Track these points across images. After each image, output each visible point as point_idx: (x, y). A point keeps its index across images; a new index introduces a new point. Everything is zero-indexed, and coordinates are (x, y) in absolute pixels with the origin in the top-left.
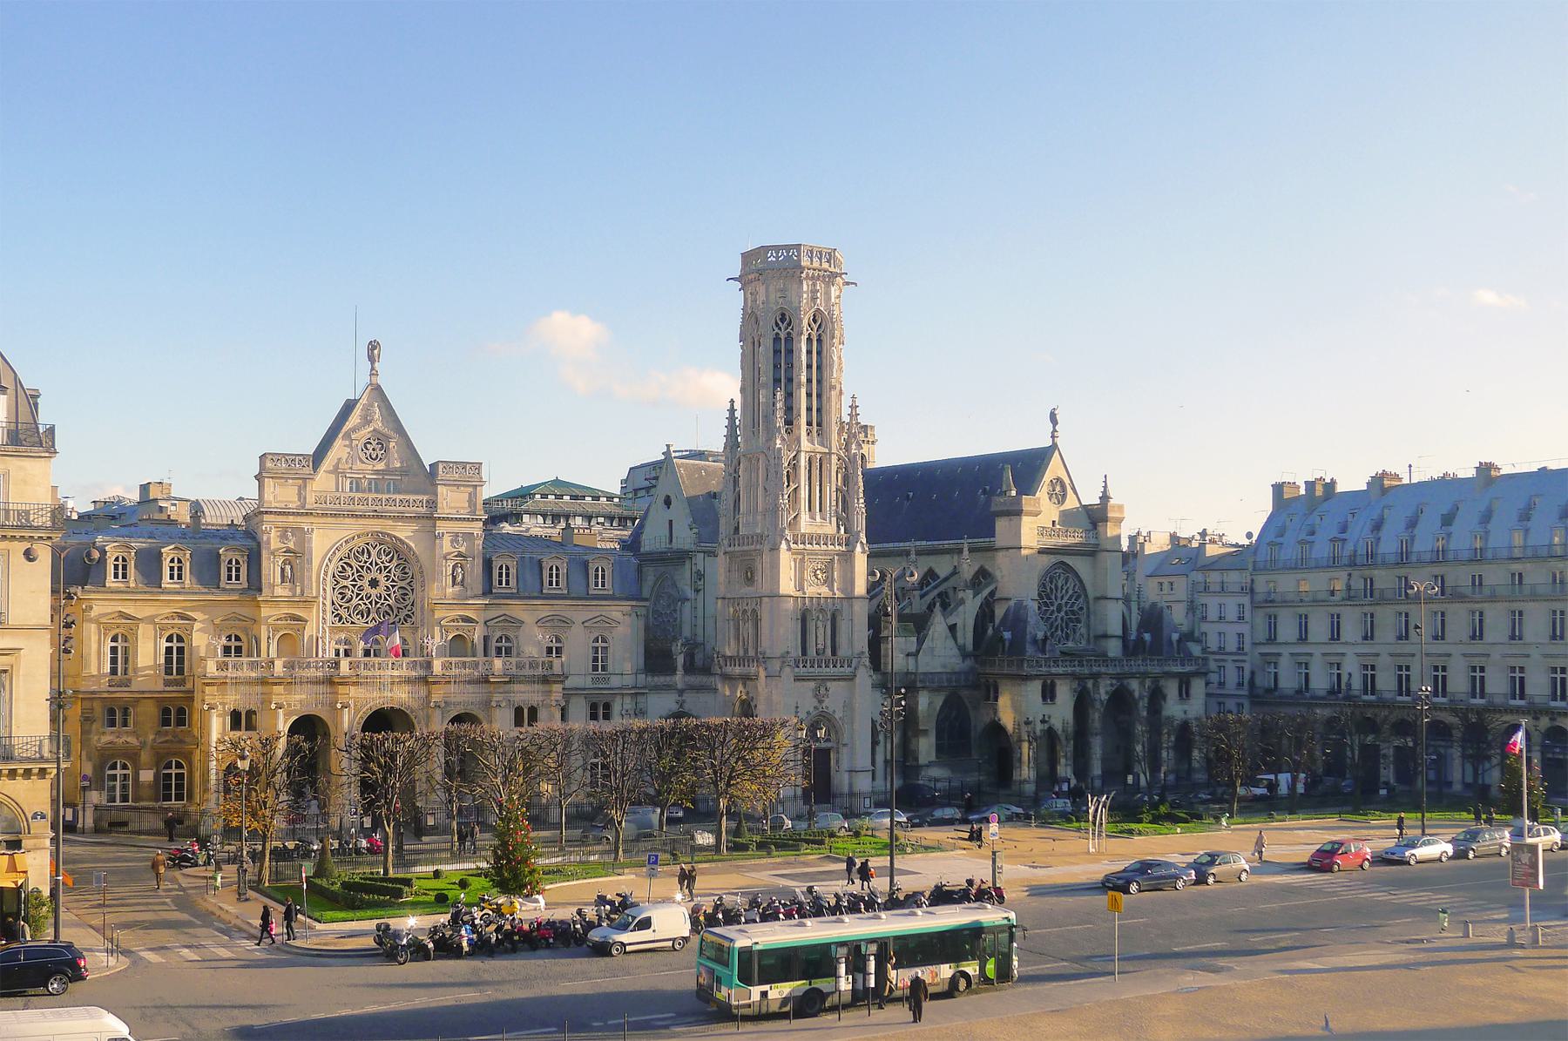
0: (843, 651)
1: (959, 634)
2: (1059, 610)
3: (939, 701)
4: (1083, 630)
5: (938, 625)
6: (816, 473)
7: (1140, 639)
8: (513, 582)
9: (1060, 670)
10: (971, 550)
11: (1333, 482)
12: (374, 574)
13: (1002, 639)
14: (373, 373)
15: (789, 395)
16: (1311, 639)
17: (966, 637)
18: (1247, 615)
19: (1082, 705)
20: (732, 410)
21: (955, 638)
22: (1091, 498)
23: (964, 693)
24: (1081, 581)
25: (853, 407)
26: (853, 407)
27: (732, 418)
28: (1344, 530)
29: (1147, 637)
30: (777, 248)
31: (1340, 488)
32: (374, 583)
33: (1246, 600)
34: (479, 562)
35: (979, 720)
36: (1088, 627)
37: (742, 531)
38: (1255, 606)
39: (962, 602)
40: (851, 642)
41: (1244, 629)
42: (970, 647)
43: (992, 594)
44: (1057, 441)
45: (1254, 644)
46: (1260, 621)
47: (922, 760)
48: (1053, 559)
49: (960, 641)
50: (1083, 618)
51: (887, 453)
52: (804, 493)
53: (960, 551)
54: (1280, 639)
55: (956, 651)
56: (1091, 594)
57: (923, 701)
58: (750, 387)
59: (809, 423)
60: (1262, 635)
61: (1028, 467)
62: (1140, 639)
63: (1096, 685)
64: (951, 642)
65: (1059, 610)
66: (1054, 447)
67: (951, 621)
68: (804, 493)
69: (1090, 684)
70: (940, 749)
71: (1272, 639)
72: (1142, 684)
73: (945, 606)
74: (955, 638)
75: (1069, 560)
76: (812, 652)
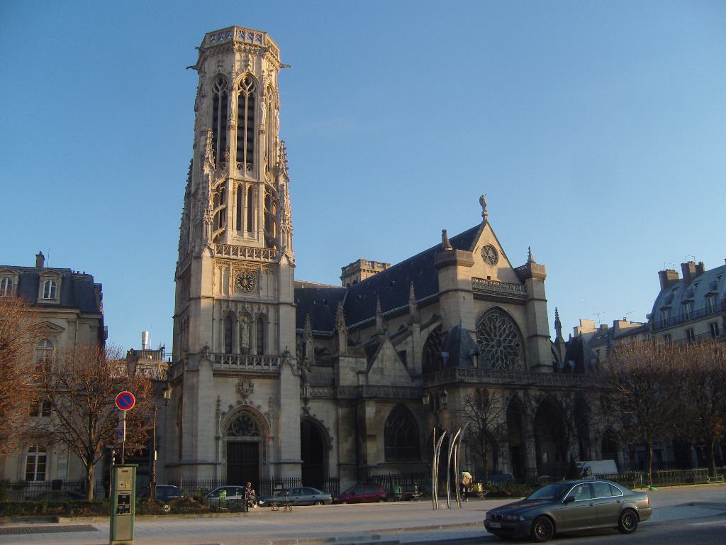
3: (387, 411)
4: (521, 363)
7: (567, 366)
9: (492, 380)
11: (701, 264)
13: (441, 358)
17: (416, 360)
19: (514, 410)
22: (519, 262)
24: (515, 324)
28: (715, 288)
29: (572, 363)
31: (707, 268)
36: (525, 359)
42: (419, 371)
43: (440, 327)
47: (371, 461)
48: (490, 305)
49: (410, 365)
50: (520, 353)
55: (405, 373)
56: (525, 335)
57: (370, 410)
62: (567, 366)
64: (399, 365)
67: (400, 348)
69: (521, 394)
74: (404, 362)
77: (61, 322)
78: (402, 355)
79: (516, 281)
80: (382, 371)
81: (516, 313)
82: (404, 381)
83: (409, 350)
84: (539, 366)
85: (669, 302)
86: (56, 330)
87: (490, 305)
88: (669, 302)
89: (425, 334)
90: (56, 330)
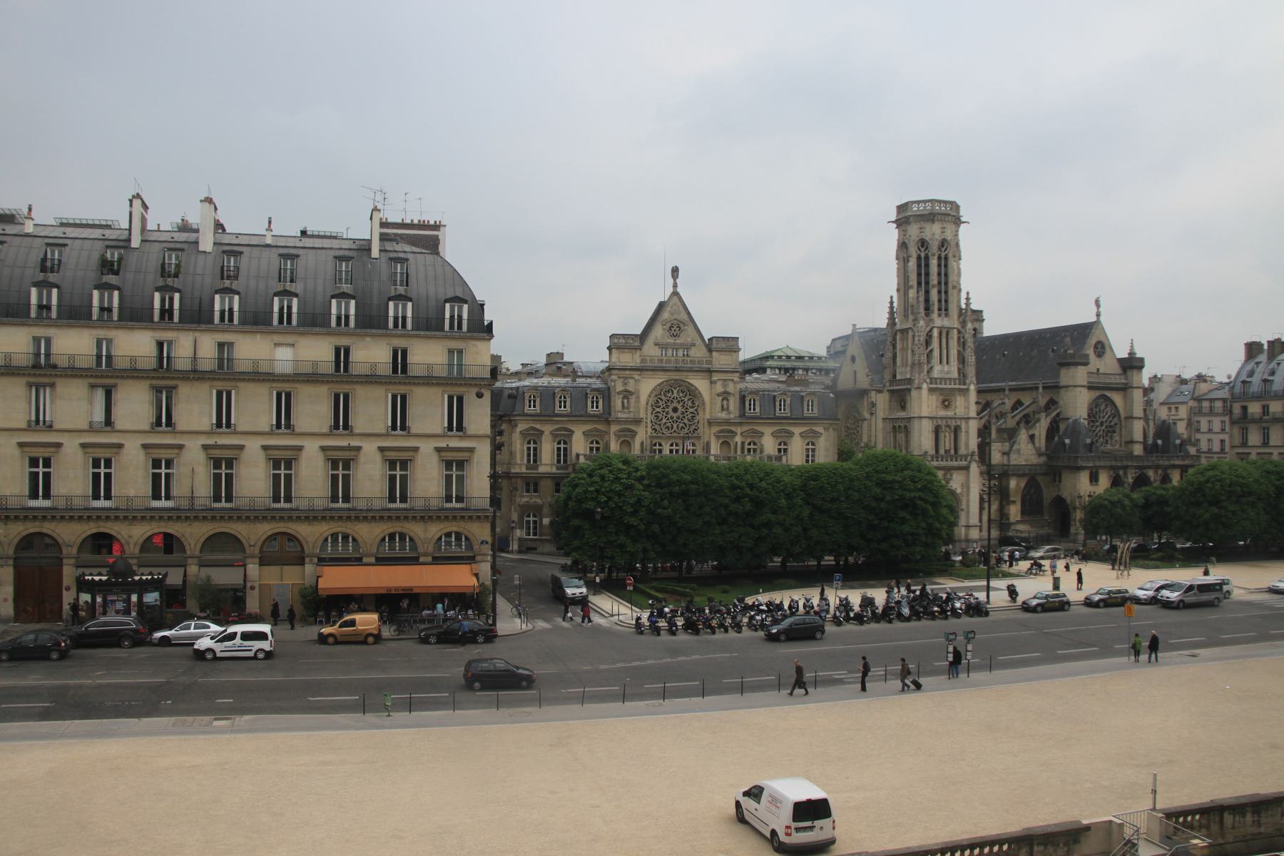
0: (962, 451)
1: (1037, 441)
2: (1102, 424)
3: (1023, 485)
5: (1023, 436)
6: (944, 341)
7: (1155, 444)
8: (758, 409)
9: (1102, 464)
10: (1044, 388)
12: (675, 404)
13: (1064, 444)
14: (675, 286)
15: (927, 292)
16: (1271, 443)
17: (1041, 442)
18: (1227, 429)
20: (892, 303)
21: (1033, 443)
22: (1122, 353)
23: (1039, 479)
25: (968, 299)
26: (968, 299)
27: (891, 307)
29: (1160, 442)
30: (918, 202)
32: (675, 410)
33: (1227, 419)
34: (737, 396)
35: (1048, 495)
37: (898, 377)
38: (1233, 423)
39: (1039, 420)
40: (967, 445)
41: (1226, 437)
42: (1043, 449)
43: (1058, 415)
44: (1102, 319)
45: (1233, 447)
46: (1236, 431)
47: (1012, 519)
48: (1098, 393)
51: (991, 328)
52: (936, 353)
53: (1037, 388)
54: (1250, 444)
56: (1123, 416)
57: (1013, 483)
58: (903, 288)
59: (940, 309)
60: (1237, 441)
61: (1082, 332)
62: (1155, 444)
63: (1125, 474)
64: (1030, 446)
65: (1102, 424)
66: (1098, 322)
68: (936, 353)
69: (1121, 473)
70: (1023, 513)
71: (1244, 444)
72: (1156, 473)
73: (1027, 422)
74: (1033, 443)
75: (1108, 394)
76: (942, 452)
77: (820, 429)
78: (1032, 437)
79: (1119, 370)
80: (1018, 451)
81: (1117, 398)
82: (1035, 460)
83: (1037, 433)
84: (1132, 442)
85: (1251, 374)
86: (817, 435)
87: (1098, 393)
88: (1251, 374)
89: (1049, 420)
90: (817, 435)
